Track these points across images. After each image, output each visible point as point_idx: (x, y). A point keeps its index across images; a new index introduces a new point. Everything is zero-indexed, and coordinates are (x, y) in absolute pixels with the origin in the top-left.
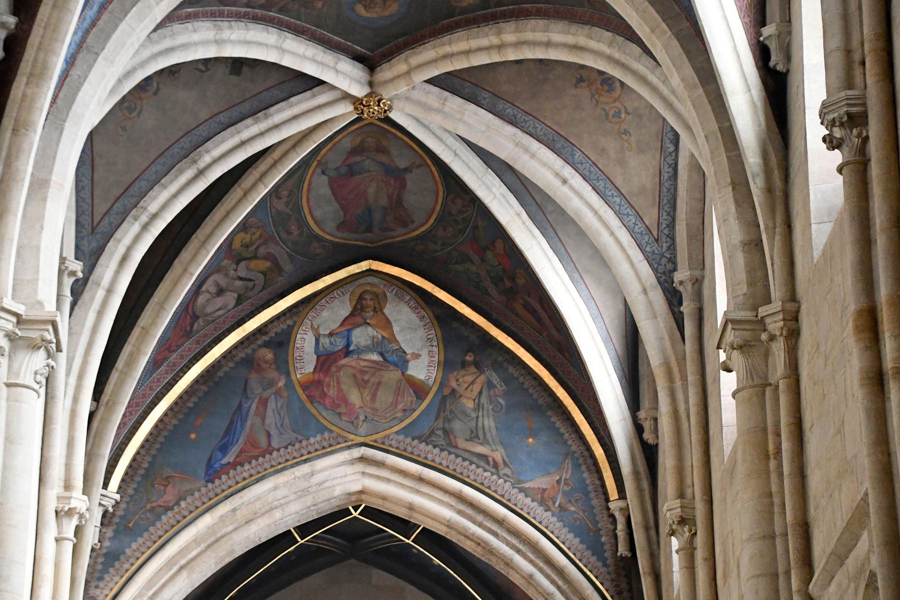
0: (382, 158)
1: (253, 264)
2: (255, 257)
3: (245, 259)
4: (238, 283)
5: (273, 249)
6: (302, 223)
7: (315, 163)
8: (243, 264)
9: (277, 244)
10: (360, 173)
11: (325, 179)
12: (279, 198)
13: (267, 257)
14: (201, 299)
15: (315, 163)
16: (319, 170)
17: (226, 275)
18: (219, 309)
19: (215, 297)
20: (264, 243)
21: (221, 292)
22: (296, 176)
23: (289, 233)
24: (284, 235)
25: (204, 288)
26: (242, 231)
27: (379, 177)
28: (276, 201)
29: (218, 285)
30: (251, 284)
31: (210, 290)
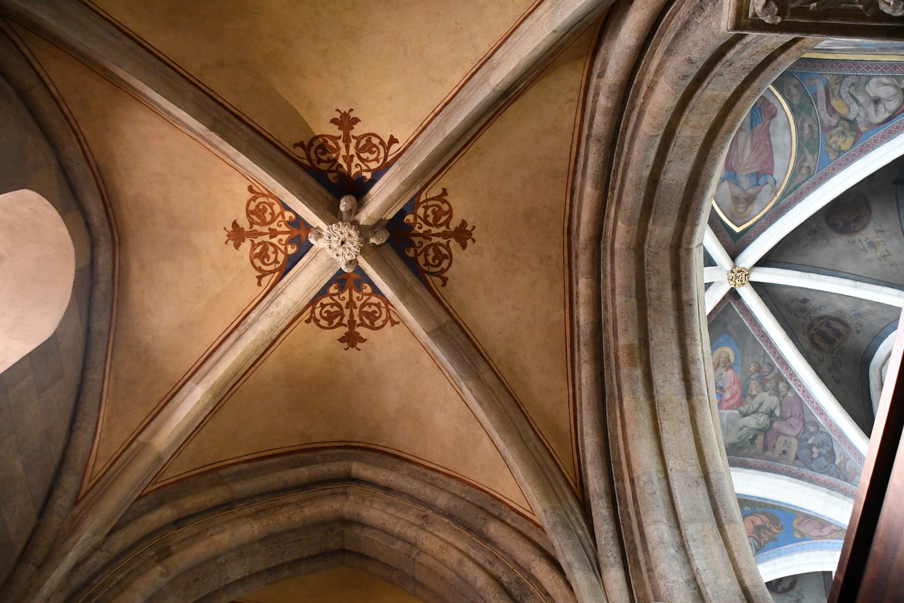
0: (737, 191)
1: (843, 111)
2: (843, 118)
3: (849, 121)
4: (861, 99)
5: (824, 115)
6: (799, 130)
7: (778, 194)
8: (851, 117)
9: (821, 120)
10: (752, 174)
11: (776, 176)
12: (808, 167)
13: (832, 111)
14: (893, 105)
15: (778, 194)
16: (778, 185)
17: (867, 115)
18: (885, 84)
19: (883, 99)
20: (831, 128)
21: (877, 101)
22: (793, 186)
23: (810, 126)
24: (815, 129)
25: (887, 115)
26: (842, 151)
27: (741, 169)
28: (812, 166)
29: (876, 110)
30: (852, 90)
31: (883, 110)
